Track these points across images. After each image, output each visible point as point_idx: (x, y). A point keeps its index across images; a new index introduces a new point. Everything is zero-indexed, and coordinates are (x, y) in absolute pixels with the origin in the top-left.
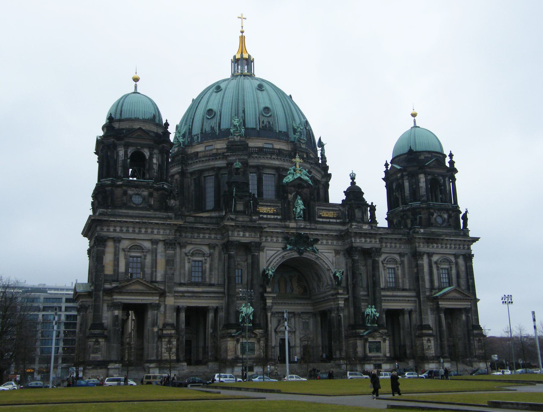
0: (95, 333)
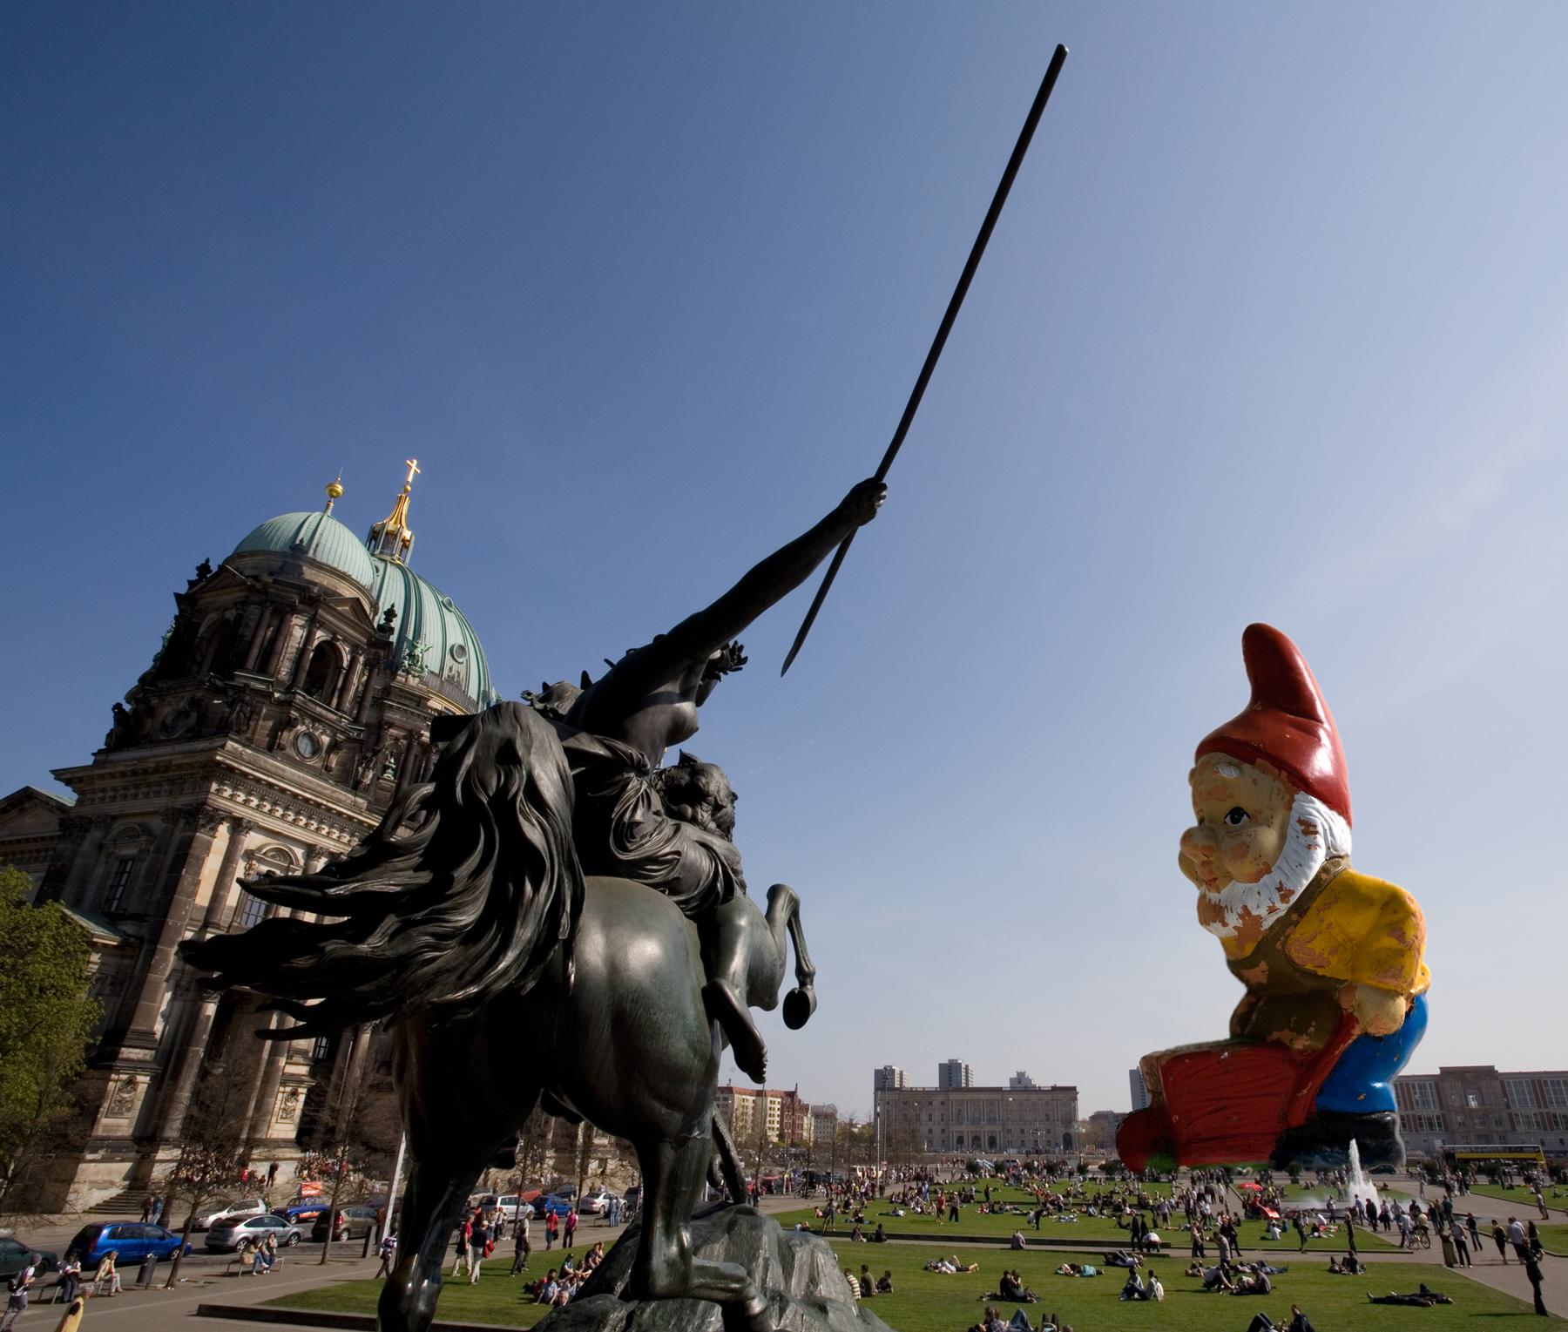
0: (132, 1056)
